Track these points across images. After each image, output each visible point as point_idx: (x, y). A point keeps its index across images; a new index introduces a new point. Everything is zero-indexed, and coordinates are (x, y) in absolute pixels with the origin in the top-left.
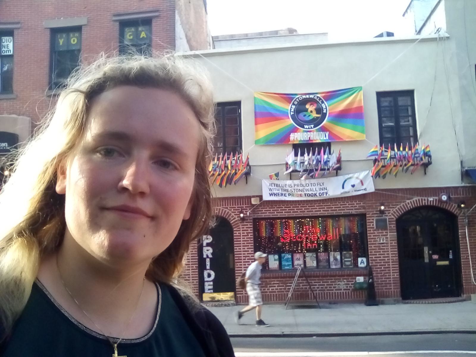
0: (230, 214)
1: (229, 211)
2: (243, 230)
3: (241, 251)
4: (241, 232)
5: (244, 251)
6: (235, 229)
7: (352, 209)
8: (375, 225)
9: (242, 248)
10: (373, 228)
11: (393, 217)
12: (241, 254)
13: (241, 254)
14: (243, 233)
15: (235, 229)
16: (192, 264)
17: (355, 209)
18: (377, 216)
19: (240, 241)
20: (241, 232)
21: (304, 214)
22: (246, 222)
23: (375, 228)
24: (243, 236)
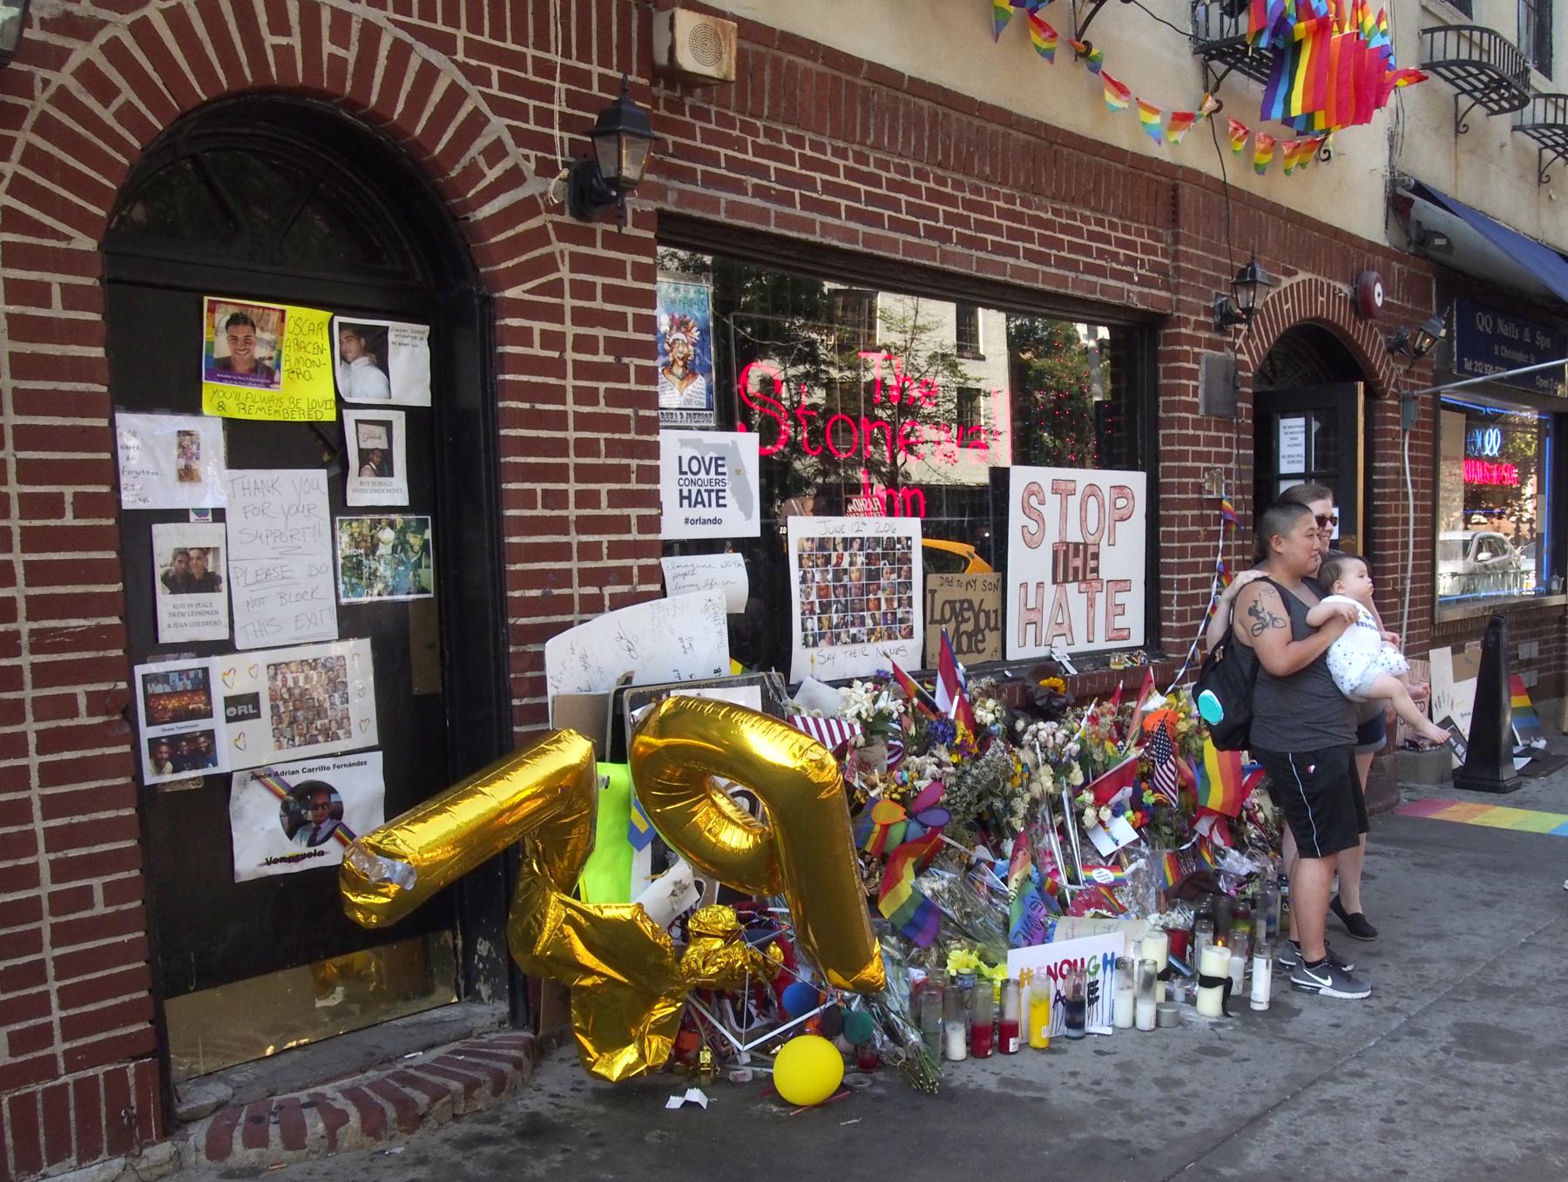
0: (476, 123)
1: (463, 82)
2: (581, 317)
3: (560, 526)
4: (570, 330)
5: (585, 525)
6: (513, 293)
7: (1127, 277)
8: (1201, 392)
9: (572, 487)
10: (1192, 407)
11: (1246, 358)
12: (562, 552)
13: (562, 552)
14: (583, 344)
15: (513, 293)
16: (43, 675)
17: (1144, 281)
18: (1210, 344)
19: (559, 421)
20: (570, 330)
21: (945, 256)
22: (611, 241)
23: (1202, 411)
24: (582, 370)
